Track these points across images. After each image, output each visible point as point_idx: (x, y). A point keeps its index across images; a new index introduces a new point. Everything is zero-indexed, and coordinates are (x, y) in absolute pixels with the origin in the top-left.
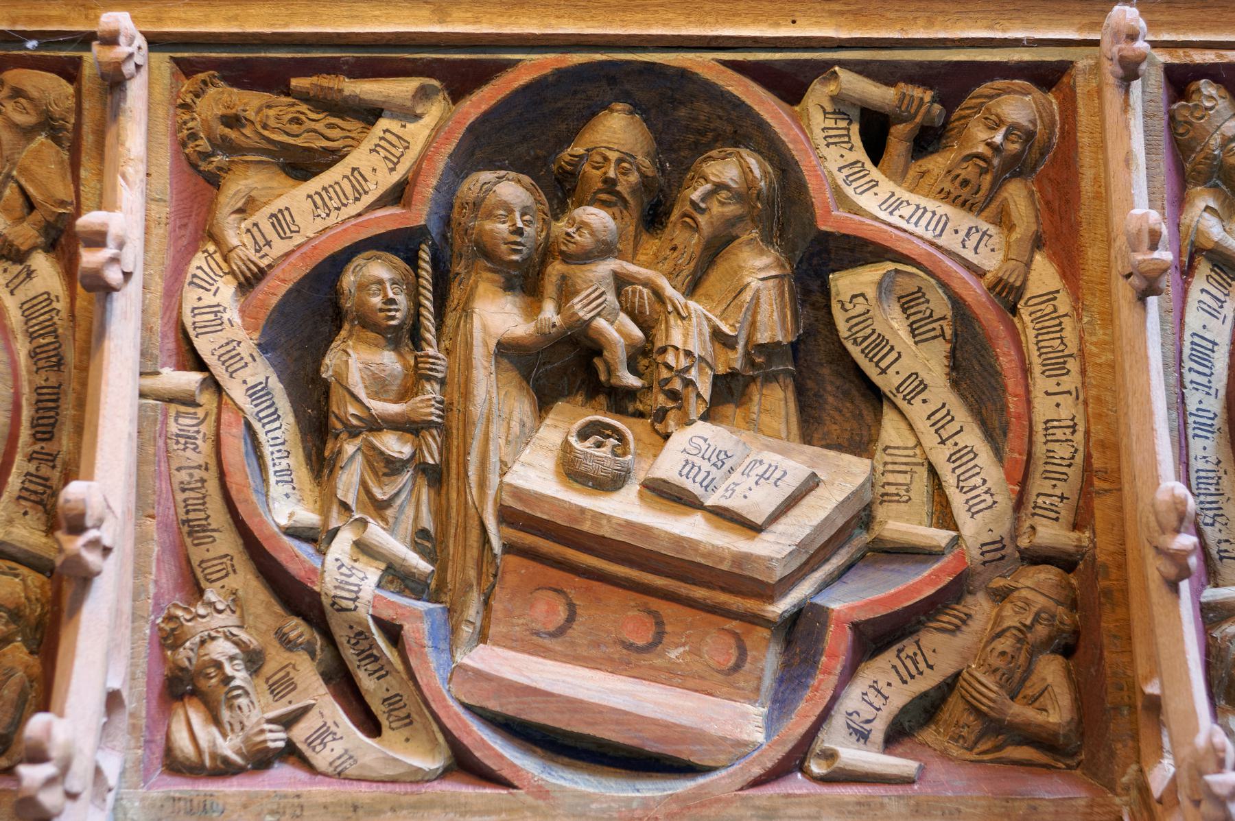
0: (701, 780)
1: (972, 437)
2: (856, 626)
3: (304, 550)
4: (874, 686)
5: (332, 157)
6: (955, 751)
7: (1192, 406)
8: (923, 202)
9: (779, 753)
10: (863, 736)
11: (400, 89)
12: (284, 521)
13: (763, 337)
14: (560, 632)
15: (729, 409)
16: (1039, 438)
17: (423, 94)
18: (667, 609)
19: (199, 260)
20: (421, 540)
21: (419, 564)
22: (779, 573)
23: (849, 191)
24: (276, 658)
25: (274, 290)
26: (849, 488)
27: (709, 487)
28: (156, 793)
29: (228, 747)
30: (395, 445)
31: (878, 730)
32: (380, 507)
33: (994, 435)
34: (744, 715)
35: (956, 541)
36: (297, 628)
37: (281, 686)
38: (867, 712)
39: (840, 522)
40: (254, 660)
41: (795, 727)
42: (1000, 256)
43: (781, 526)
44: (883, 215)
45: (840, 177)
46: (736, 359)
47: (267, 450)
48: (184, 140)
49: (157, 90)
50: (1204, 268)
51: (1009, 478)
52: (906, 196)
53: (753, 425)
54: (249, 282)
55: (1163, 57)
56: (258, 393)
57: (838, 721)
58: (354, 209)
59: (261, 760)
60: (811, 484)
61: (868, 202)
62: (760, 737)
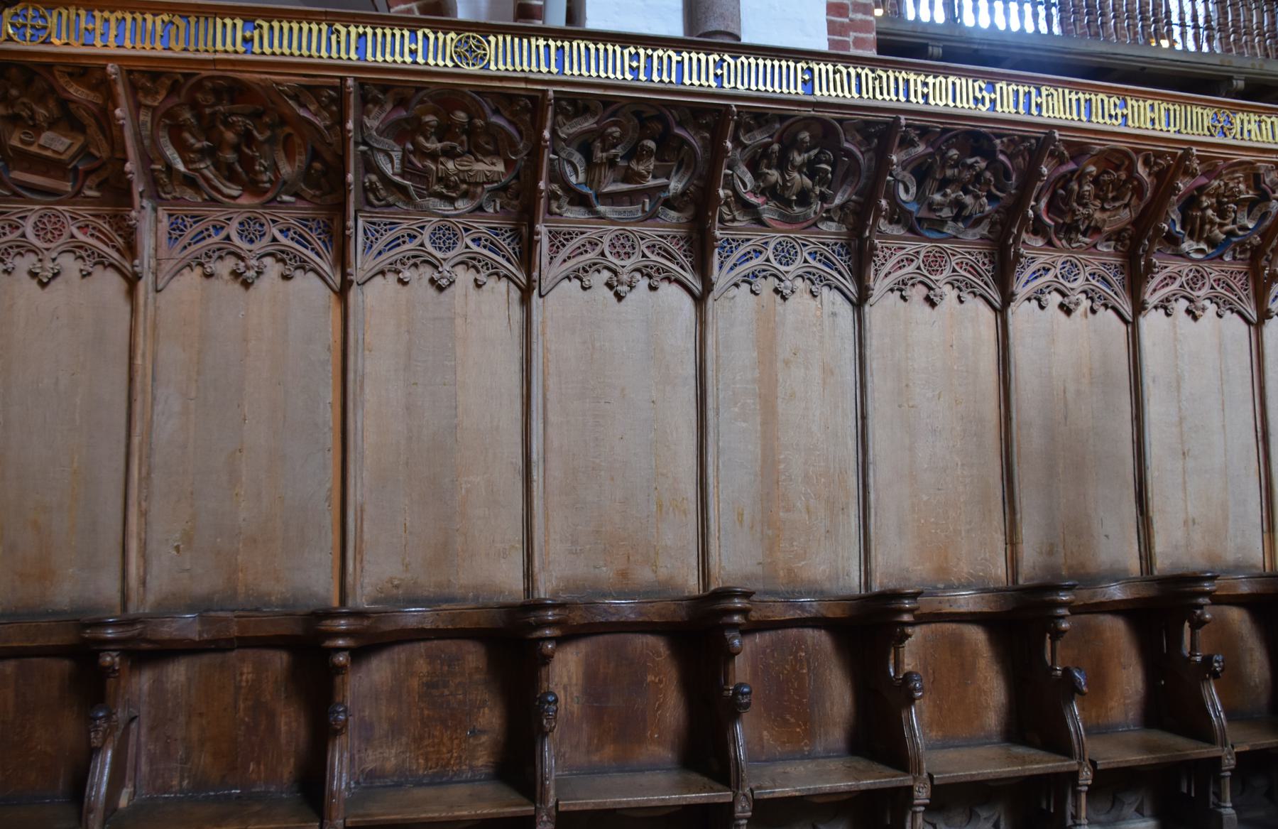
0: (62, 197)
1: (101, 137)
10: (90, 188)
23: (67, 88)
27: (51, 145)
31: (94, 186)
33: (105, 137)
34: (67, 186)
41: (76, 188)
43: (67, 153)
45: (64, 85)
55: (125, 68)
57: (85, 187)
60: (71, 145)
61: (71, 91)
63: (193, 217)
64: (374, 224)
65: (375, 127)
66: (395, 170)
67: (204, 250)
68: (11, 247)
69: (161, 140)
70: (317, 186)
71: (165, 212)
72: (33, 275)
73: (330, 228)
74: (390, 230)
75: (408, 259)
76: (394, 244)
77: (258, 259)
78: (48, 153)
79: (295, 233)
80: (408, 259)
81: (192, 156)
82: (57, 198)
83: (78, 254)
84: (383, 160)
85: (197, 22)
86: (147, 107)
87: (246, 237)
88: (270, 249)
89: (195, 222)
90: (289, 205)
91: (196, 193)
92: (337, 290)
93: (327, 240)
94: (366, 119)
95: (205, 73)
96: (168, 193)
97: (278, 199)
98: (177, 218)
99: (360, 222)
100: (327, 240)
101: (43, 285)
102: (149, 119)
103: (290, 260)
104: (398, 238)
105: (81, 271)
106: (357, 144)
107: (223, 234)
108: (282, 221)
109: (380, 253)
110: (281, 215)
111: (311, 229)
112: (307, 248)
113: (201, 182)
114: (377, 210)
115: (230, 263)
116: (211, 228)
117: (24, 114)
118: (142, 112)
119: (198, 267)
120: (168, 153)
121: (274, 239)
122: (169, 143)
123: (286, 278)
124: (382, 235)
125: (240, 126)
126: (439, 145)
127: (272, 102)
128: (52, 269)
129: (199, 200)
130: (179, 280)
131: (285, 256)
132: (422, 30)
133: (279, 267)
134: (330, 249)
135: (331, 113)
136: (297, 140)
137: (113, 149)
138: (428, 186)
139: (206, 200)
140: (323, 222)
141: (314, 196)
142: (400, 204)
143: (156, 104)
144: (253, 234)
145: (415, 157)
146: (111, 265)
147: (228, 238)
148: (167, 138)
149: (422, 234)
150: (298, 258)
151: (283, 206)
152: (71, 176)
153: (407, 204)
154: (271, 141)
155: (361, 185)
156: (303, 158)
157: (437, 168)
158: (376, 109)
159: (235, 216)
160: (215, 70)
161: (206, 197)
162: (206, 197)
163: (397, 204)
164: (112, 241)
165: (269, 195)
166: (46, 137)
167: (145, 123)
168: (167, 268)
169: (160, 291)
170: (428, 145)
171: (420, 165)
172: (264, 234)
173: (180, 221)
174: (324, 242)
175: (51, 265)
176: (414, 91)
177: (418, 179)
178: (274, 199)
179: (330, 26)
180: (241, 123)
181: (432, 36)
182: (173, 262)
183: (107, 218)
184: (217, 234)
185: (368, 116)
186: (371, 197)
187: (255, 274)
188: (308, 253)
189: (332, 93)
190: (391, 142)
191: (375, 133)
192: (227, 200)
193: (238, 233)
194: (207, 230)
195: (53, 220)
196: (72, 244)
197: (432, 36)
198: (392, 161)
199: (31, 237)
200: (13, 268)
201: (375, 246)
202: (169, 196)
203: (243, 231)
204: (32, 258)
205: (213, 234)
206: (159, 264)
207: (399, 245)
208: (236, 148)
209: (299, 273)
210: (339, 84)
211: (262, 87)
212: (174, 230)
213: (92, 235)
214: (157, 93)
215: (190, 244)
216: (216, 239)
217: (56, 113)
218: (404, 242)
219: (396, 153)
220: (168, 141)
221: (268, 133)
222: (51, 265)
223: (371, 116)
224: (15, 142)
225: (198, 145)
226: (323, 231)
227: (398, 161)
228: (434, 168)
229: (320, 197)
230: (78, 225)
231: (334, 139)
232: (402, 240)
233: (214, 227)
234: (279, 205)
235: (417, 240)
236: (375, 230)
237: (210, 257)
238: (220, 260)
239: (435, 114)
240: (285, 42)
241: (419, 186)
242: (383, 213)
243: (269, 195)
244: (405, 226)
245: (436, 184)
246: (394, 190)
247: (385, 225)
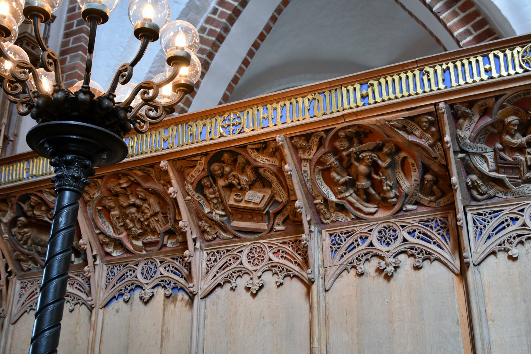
0: (262, 234)
1: (281, 188)
2: (274, 214)
3: (210, 214)
4: (279, 219)
5: (195, 166)
6: (291, 224)
7: (306, 180)
8: (266, 158)
9: (269, 230)
10: (279, 225)
11: (198, 158)
12: (206, 212)
13: (252, 180)
14: (241, 218)
15: (252, 187)
16: (289, 186)
17: (201, 158)
18: (253, 214)
19: (185, 182)
20: (223, 210)
21: (223, 213)
22: (263, 209)
24: (213, 226)
25: (195, 185)
26: (269, 195)
28: (205, 244)
29: (210, 238)
30: (215, 201)
31: (281, 223)
32: (216, 209)
33: (283, 187)
34: (265, 225)
35: (282, 201)
36: (213, 223)
37: (214, 229)
38: (279, 222)
39: (269, 199)
40: (210, 227)
42: (278, 163)
43: (262, 203)
44: (261, 162)
46: (250, 183)
47: (202, 203)
48: (177, 170)
49: (171, 165)
50: (303, 161)
51: (286, 193)
52: (264, 158)
53: (256, 188)
54: (192, 184)
55: (288, 136)
56: (198, 197)
57: (275, 224)
58: (200, 173)
59: (214, 239)
60: (264, 197)
61: (259, 160)
62: (267, 228)
63: (345, 234)
64: (481, 214)
65: (468, 136)
66: (490, 167)
67: (355, 256)
68: (234, 272)
69: (318, 181)
70: (432, 193)
71: (327, 233)
72: (248, 289)
73: (446, 224)
74: (495, 217)
75: (514, 238)
76: (500, 228)
77: (394, 257)
78: (251, 205)
79: (420, 233)
80: (514, 238)
81: (339, 188)
82: (260, 235)
83: (274, 271)
84: (478, 160)
85: (330, 94)
86: (306, 160)
87: (384, 241)
88: (402, 248)
89: (347, 237)
90: (413, 212)
91: (346, 216)
92: (458, 272)
93: (444, 234)
94: (459, 132)
95: (338, 127)
96: (328, 219)
97: (404, 209)
98: (336, 236)
99: (469, 215)
100: (444, 234)
101: (254, 295)
102: (308, 168)
103: (419, 254)
104: (503, 223)
105: (277, 282)
106: (456, 153)
107: (367, 242)
108: (409, 225)
109: (489, 237)
110: (408, 221)
111: (431, 228)
112: (430, 243)
113: (348, 206)
114: (481, 203)
115: (375, 263)
116: (359, 239)
117: (234, 182)
118: (303, 164)
119: (353, 269)
120: (323, 190)
121: (405, 240)
122: (323, 183)
123: (417, 268)
124: (488, 222)
125: (368, 159)
126: (524, 139)
127: (388, 136)
128: (259, 283)
129: (349, 220)
130: (340, 281)
131: (414, 251)
132: (493, 52)
133: (411, 261)
134: (448, 241)
135: (432, 134)
136: (411, 161)
137: (289, 195)
138: (521, 174)
139: (353, 219)
140: (440, 220)
141: (430, 201)
142: (500, 195)
143: (311, 157)
144: (389, 238)
145: (505, 153)
146: (295, 276)
147: (371, 244)
148: (322, 179)
149: (523, 216)
150: (424, 252)
151: (408, 213)
152: (266, 218)
153: (506, 194)
154: (392, 166)
155: (465, 185)
156: (417, 173)
157: (526, 159)
158: (467, 122)
159: (374, 227)
160: (345, 122)
161: (354, 217)
162: (354, 217)
163: (497, 195)
164: (294, 259)
165: (397, 207)
166: (249, 195)
167: (306, 172)
168: (332, 273)
169: (328, 291)
170: (513, 141)
171: (510, 159)
172: (397, 237)
173: (337, 237)
174: (443, 236)
175: (258, 281)
176: (494, 100)
177: (511, 171)
178: (401, 210)
179: (421, 70)
180: (368, 157)
181: (501, 55)
182: (334, 268)
183: (291, 243)
184: (363, 243)
185: (461, 129)
186: (475, 193)
187: (393, 269)
188: (432, 246)
189: (429, 117)
190: (483, 145)
191: (469, 141)
192: (367, 216)
193: (378, 239)
194: (356, 241)
195: (258, 250)
196: (270, 265)
197: (501, 55)
198: (486, 161)
199: (246, 264)
200: (236, 286)
201: (484, 232)
202: (328, 221)
203: (381, 237)
204: (246, 278)
205: (361, 244)
206: (325, 271)
207: (504, 228)
208: (368, 177)
209: (427, 262)
210: (434, 110)
211: (378, 127)
212: (334, 244)
213: (282, 257)
214: (310, 149)
215: (345, 254)
216: (363, 246)
217: (253, 178)
218: (508, 225)
219: (489, 154)
220: (323, 182)
221: (389, 160)
222: (258, 281)
223: (463, 129)
224: (232, 202)
225: (342, 180)
226: (441, 227)
227: (492, 160)
228: (523, 159)
229: (435, 201)
230: (273, 251)
231: (438, 153)
232: (506, 223)
233: (361, 238)
234: (406, 213)
235: (519, 221)
236: (482, 219)
237: (360, 261)
238: (367, 262)
239: (515, 114)
240: (391, 90)
241: (514, 176)
242: (487, 204)
243: (397, 207)
244: (506, 212)
245: (528, 172)
246: (493, 184)
247: (490, 214)
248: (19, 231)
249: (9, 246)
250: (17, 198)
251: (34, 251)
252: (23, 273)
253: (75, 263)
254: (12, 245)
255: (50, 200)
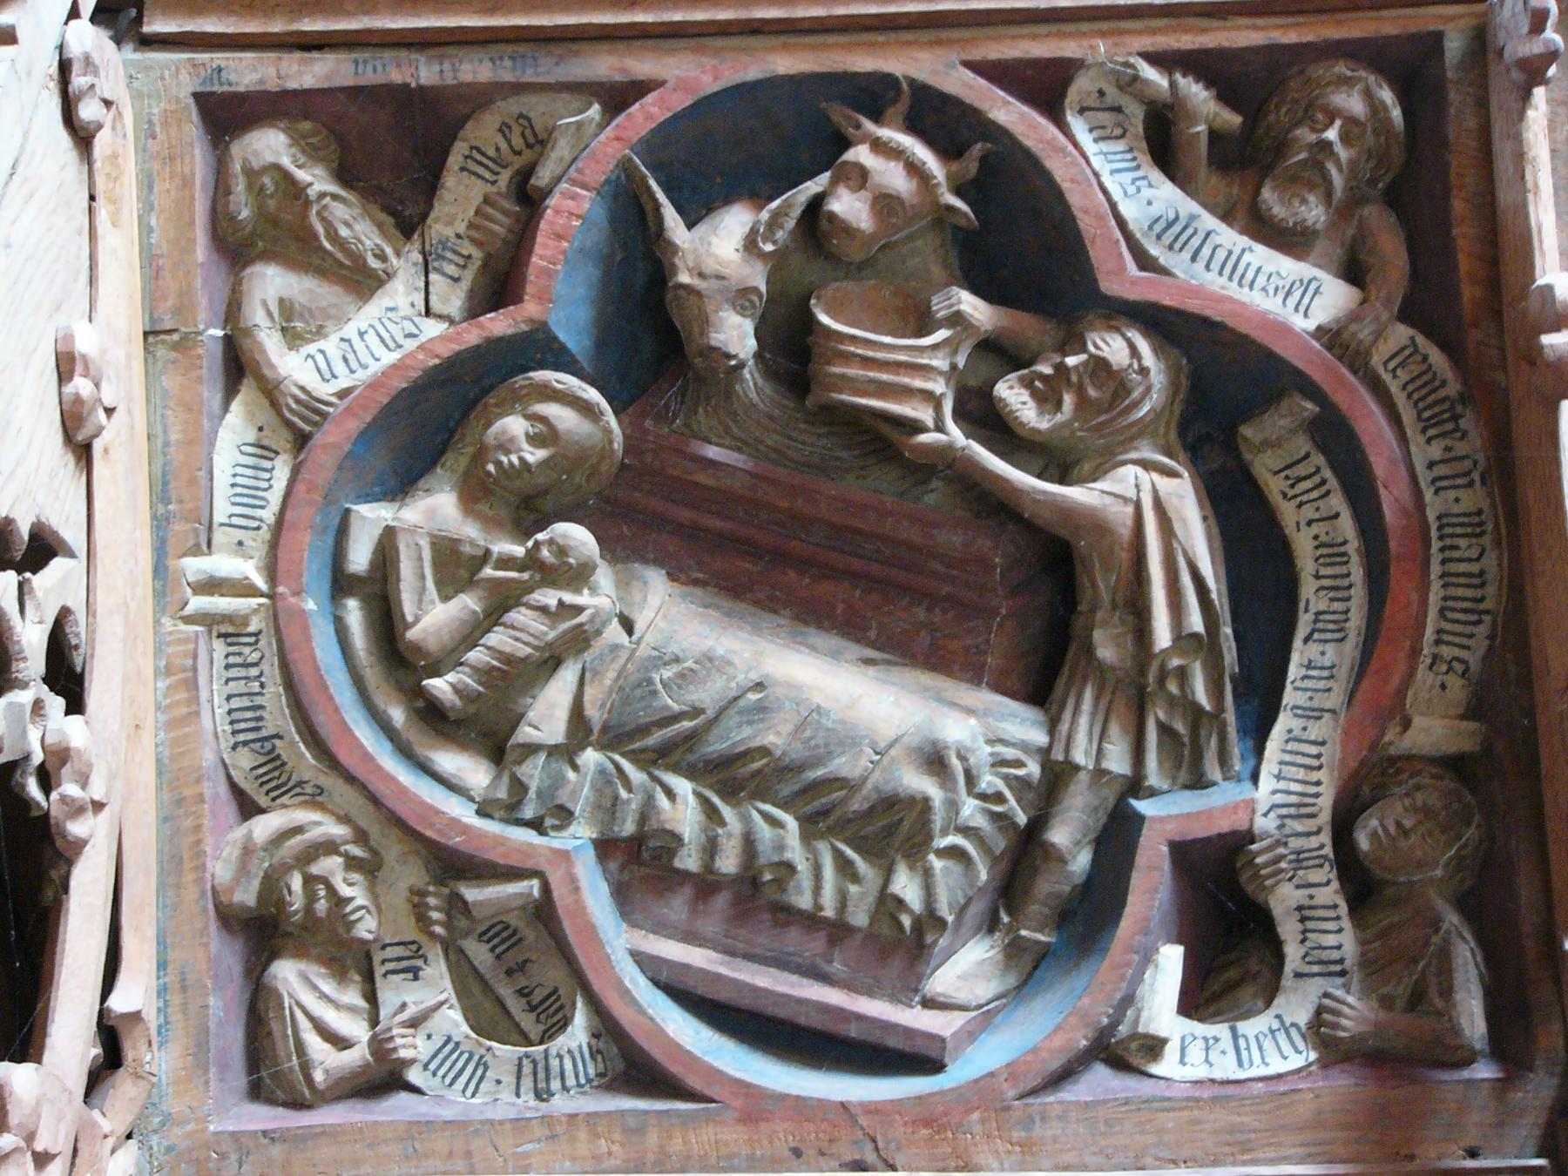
248: (470, 532)
249: (214, 714)
250: (646, 115)
251: (579, 836)
252: (263, 1117)
253: (1166, 1066)
254: (274, 696)
255: (1128, 210)
